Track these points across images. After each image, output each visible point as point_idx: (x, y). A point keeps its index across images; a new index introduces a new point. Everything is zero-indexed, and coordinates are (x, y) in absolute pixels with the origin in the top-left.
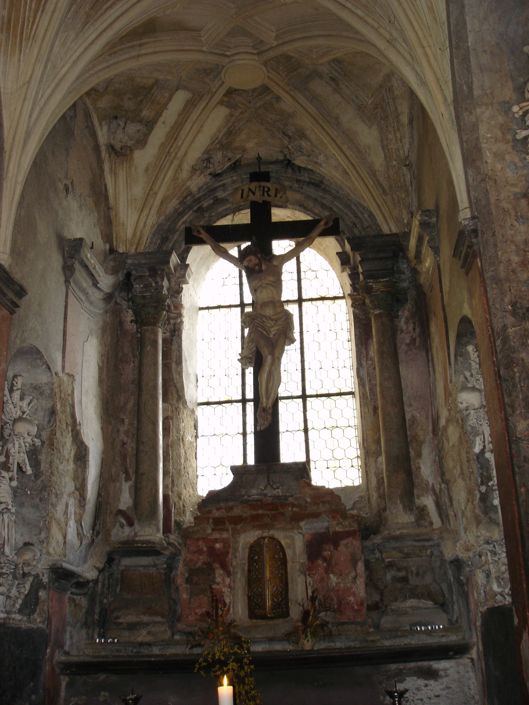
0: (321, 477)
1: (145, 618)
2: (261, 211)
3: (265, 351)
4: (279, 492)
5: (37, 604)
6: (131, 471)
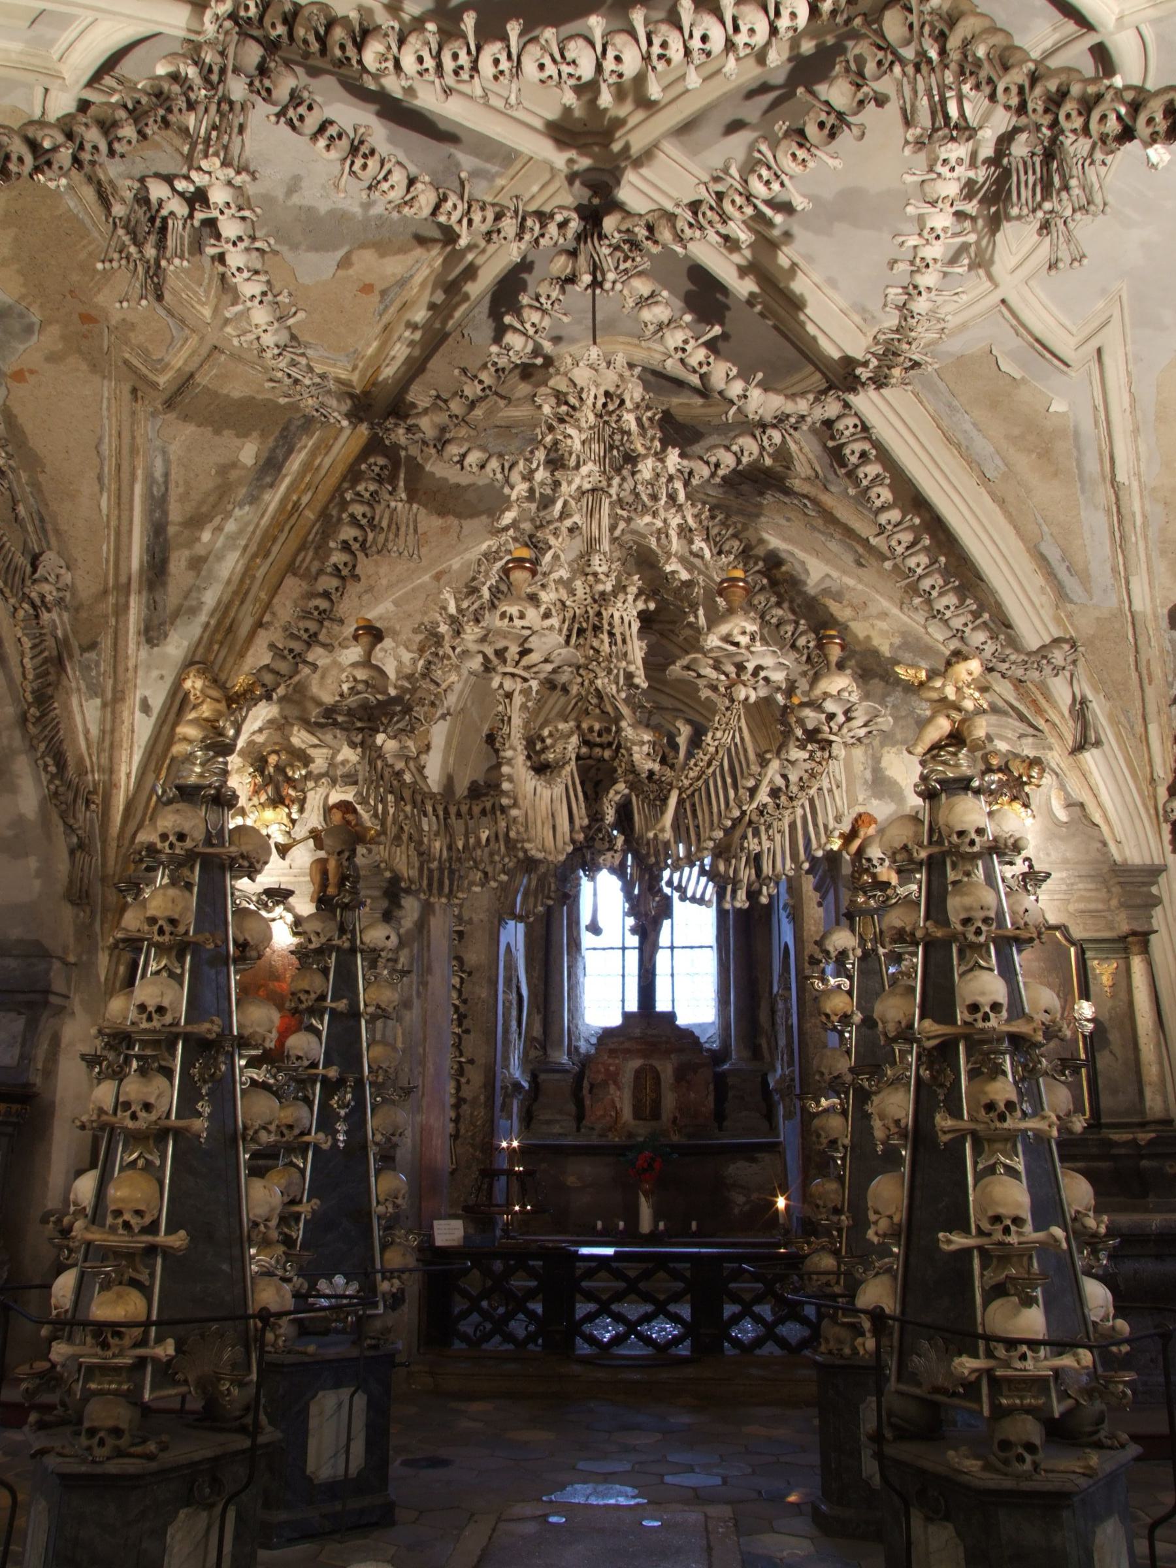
1: (558, 1117)
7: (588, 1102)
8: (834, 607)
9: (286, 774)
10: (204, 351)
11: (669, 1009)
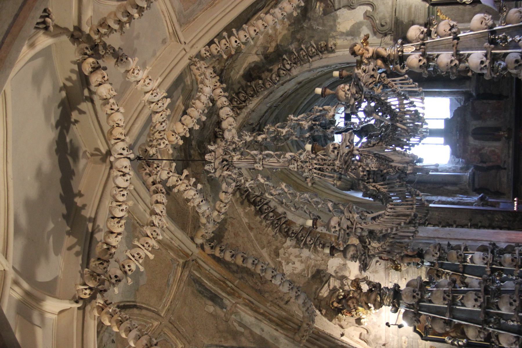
6: (439, 186)
7: (491, 164)
8: (271, 50)
9: (342, 299)
10: (170, 326)
11: (443, 122)
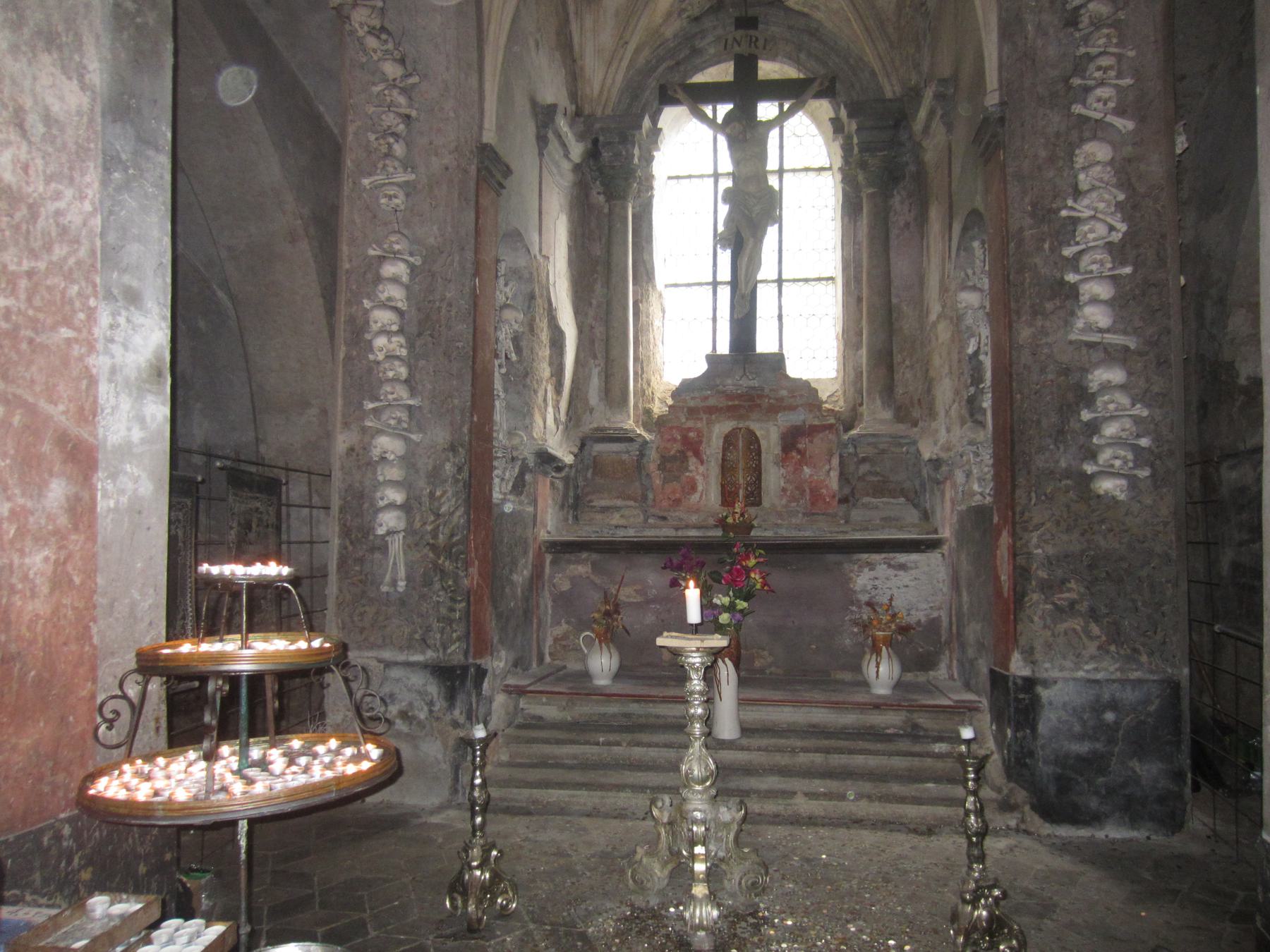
0: (794, 369)
1: (619, 503)
2: (746, 66)
3: (746, 233)
4: (755, 383)
5: (524, 486)
11: (773, 348)
